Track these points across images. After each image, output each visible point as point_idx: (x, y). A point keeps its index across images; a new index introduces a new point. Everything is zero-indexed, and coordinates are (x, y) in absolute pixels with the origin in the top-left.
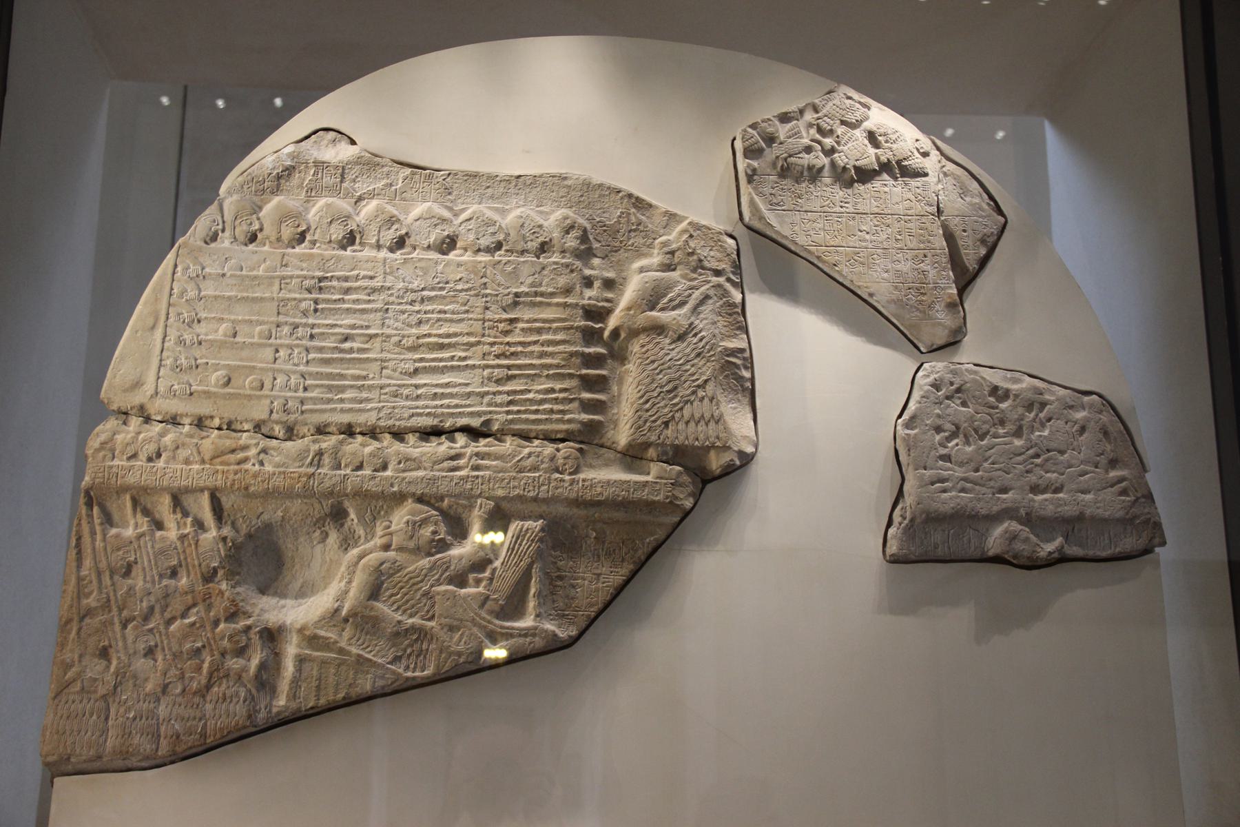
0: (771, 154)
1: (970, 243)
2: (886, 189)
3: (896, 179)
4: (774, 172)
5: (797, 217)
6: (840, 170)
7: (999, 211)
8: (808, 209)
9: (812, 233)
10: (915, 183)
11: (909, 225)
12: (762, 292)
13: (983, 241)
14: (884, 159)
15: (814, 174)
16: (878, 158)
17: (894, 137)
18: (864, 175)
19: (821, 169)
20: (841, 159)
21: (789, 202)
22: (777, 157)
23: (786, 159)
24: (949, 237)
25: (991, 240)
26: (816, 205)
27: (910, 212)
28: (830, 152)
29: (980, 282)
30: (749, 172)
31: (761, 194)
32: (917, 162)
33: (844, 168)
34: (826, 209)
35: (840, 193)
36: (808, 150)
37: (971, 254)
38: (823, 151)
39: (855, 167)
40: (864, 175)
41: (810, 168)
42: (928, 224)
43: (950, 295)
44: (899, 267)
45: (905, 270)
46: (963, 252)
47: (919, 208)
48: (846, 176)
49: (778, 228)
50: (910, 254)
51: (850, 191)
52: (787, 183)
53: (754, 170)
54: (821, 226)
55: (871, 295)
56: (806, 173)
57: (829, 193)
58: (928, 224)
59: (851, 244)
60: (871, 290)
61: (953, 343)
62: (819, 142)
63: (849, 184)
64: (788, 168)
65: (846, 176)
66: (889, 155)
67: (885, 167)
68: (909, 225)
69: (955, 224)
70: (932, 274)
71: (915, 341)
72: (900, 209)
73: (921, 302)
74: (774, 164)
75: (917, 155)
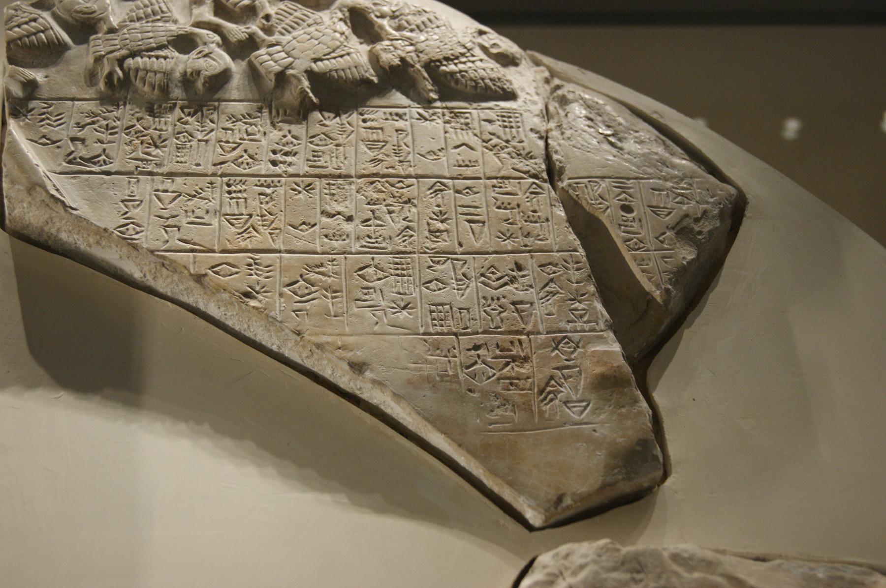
0: (81, 57)
1: (646, 233)
2: (400, 124)
3: (427, 103)
4: (91, 93)
5: (144, 187)
6: (270, 82)
7: (713, 170)
8: (180, 168)
9: (183, 221)
10: (475, 112)
11: (466, 199)
12: (30, 384)
13: (683, 231)
14: (390, 57)
15: (204, 94)
16: (374, 59)
17: (418, 20)
18: (337, 94)
19: (222, 78)
20: (269, 60)
21: (121, 154)
22: (98, 60)
23: (121, 61)
24: (585, 224)
25: (706, 227)
26: (204, 157)
27: (468, 172)
28: (243, 49)
29: (691, 338)
30: (17, 91)
31: (46, 141)
32: (484, 68)
33: (282, 78)
34: (231, 168)
35: (269, 135)
36: (185, 43)
37: (651, 268)
38: (226, 44)
39: (310, 73)
40: (337, 94)
41: (188, 80)
42: (521, 197)
43: (600, 358)
44: (442, 295)
45: (460, 300)
46: (627, 255)
47: (492, 162)
48: (290, 96)
49: (84, 210)
50: (474, 264)
51: (298, 129)
52: (126, 114)
53: (31, 86)
54: (214, 204)
55: (358, 367)
56: (177, 92)
57: (244, 134)
58: (521, 197)
59: (300, 245)
60: (359, 355)
61: (627, 491)
62: (216, 29)
63: (301, 112)
64: (126, 82)
65: (290, 96)
66: (405, 50)
67: (396, 77)
68: (466, 199)
69: (600, 199)
70: (543, 311)
71: (507, 494)
72: (444, 165)
73: (512, 381)
74: (91, 77)
75: (478, 52)
